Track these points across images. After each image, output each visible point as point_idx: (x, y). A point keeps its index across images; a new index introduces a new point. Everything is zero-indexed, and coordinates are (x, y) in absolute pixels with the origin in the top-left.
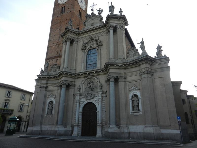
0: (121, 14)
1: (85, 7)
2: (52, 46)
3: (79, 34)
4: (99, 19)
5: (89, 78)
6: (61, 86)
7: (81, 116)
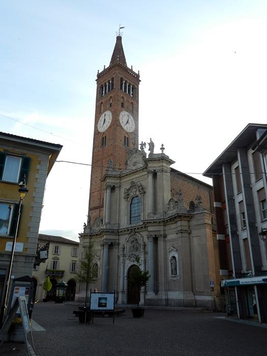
0: (163, 151)
3: (120, 177)
4: (142, 156)
5: (132, 235)
6: (103, 245)
7: (126, 281)
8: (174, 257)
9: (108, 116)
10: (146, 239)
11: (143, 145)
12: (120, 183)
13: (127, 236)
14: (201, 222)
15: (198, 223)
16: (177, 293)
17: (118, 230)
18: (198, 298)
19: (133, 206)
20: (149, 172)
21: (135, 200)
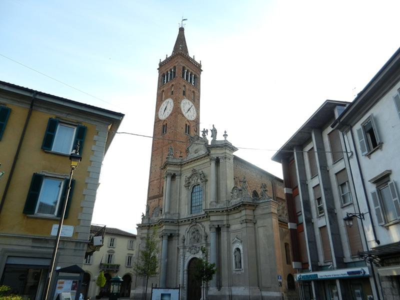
0: (225, 138)
2: (153, 181)
3: (181, 165)
5: (194, 225)
6: (162, 237)
7: (186, 276)
8: (238, 249)
9: (169, 104)
10: (207, 230)
11: (205, 132)
12: (181, 171)
13: (187, 227)
14: (267, 211)
15: (264, 213)
16: (242, 288)
17: (177, 220)
18: (265, 294)
19: (194, 195)
20: (211, 159)
21: (197, 189)
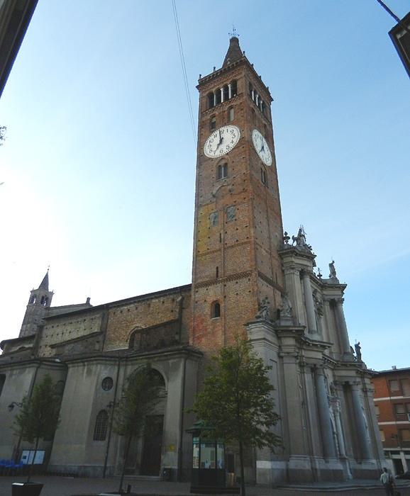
1: (270, 159)
